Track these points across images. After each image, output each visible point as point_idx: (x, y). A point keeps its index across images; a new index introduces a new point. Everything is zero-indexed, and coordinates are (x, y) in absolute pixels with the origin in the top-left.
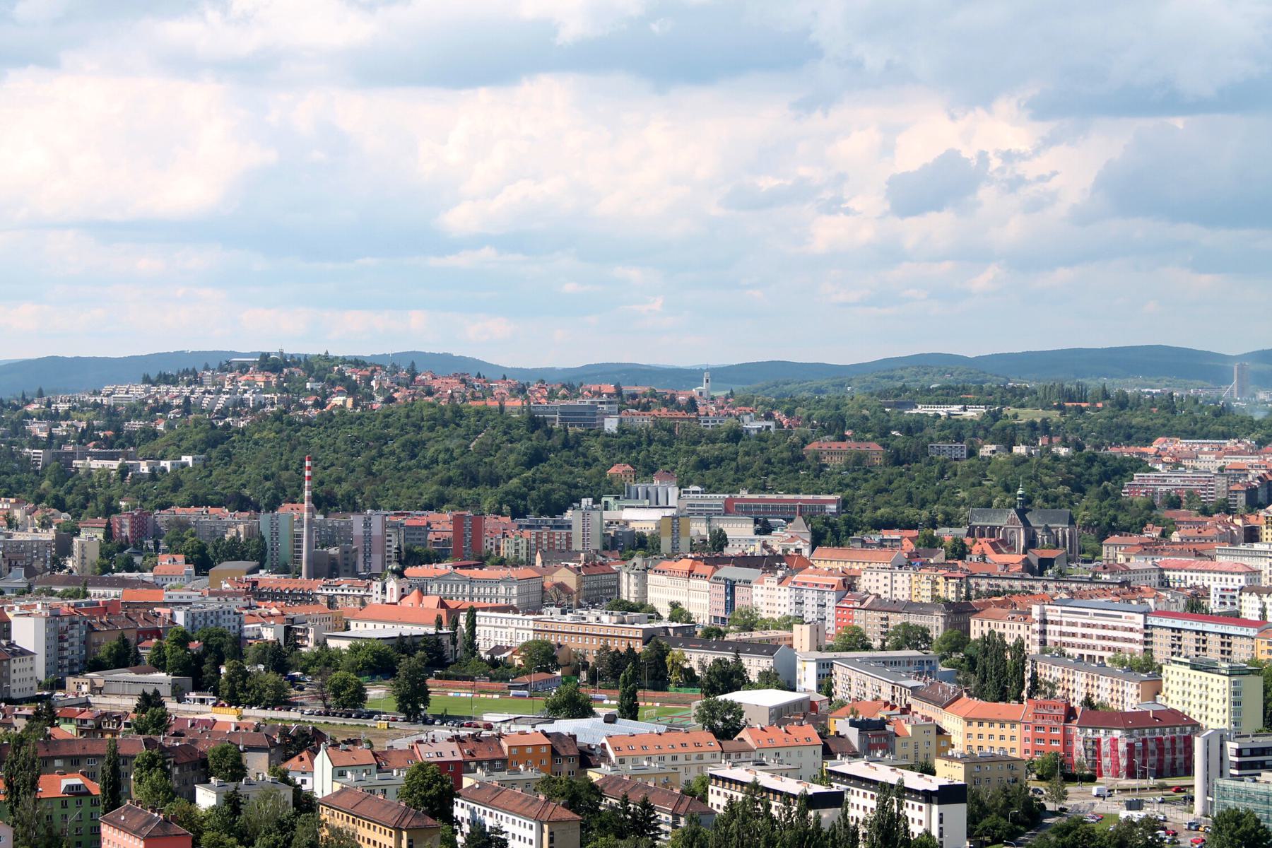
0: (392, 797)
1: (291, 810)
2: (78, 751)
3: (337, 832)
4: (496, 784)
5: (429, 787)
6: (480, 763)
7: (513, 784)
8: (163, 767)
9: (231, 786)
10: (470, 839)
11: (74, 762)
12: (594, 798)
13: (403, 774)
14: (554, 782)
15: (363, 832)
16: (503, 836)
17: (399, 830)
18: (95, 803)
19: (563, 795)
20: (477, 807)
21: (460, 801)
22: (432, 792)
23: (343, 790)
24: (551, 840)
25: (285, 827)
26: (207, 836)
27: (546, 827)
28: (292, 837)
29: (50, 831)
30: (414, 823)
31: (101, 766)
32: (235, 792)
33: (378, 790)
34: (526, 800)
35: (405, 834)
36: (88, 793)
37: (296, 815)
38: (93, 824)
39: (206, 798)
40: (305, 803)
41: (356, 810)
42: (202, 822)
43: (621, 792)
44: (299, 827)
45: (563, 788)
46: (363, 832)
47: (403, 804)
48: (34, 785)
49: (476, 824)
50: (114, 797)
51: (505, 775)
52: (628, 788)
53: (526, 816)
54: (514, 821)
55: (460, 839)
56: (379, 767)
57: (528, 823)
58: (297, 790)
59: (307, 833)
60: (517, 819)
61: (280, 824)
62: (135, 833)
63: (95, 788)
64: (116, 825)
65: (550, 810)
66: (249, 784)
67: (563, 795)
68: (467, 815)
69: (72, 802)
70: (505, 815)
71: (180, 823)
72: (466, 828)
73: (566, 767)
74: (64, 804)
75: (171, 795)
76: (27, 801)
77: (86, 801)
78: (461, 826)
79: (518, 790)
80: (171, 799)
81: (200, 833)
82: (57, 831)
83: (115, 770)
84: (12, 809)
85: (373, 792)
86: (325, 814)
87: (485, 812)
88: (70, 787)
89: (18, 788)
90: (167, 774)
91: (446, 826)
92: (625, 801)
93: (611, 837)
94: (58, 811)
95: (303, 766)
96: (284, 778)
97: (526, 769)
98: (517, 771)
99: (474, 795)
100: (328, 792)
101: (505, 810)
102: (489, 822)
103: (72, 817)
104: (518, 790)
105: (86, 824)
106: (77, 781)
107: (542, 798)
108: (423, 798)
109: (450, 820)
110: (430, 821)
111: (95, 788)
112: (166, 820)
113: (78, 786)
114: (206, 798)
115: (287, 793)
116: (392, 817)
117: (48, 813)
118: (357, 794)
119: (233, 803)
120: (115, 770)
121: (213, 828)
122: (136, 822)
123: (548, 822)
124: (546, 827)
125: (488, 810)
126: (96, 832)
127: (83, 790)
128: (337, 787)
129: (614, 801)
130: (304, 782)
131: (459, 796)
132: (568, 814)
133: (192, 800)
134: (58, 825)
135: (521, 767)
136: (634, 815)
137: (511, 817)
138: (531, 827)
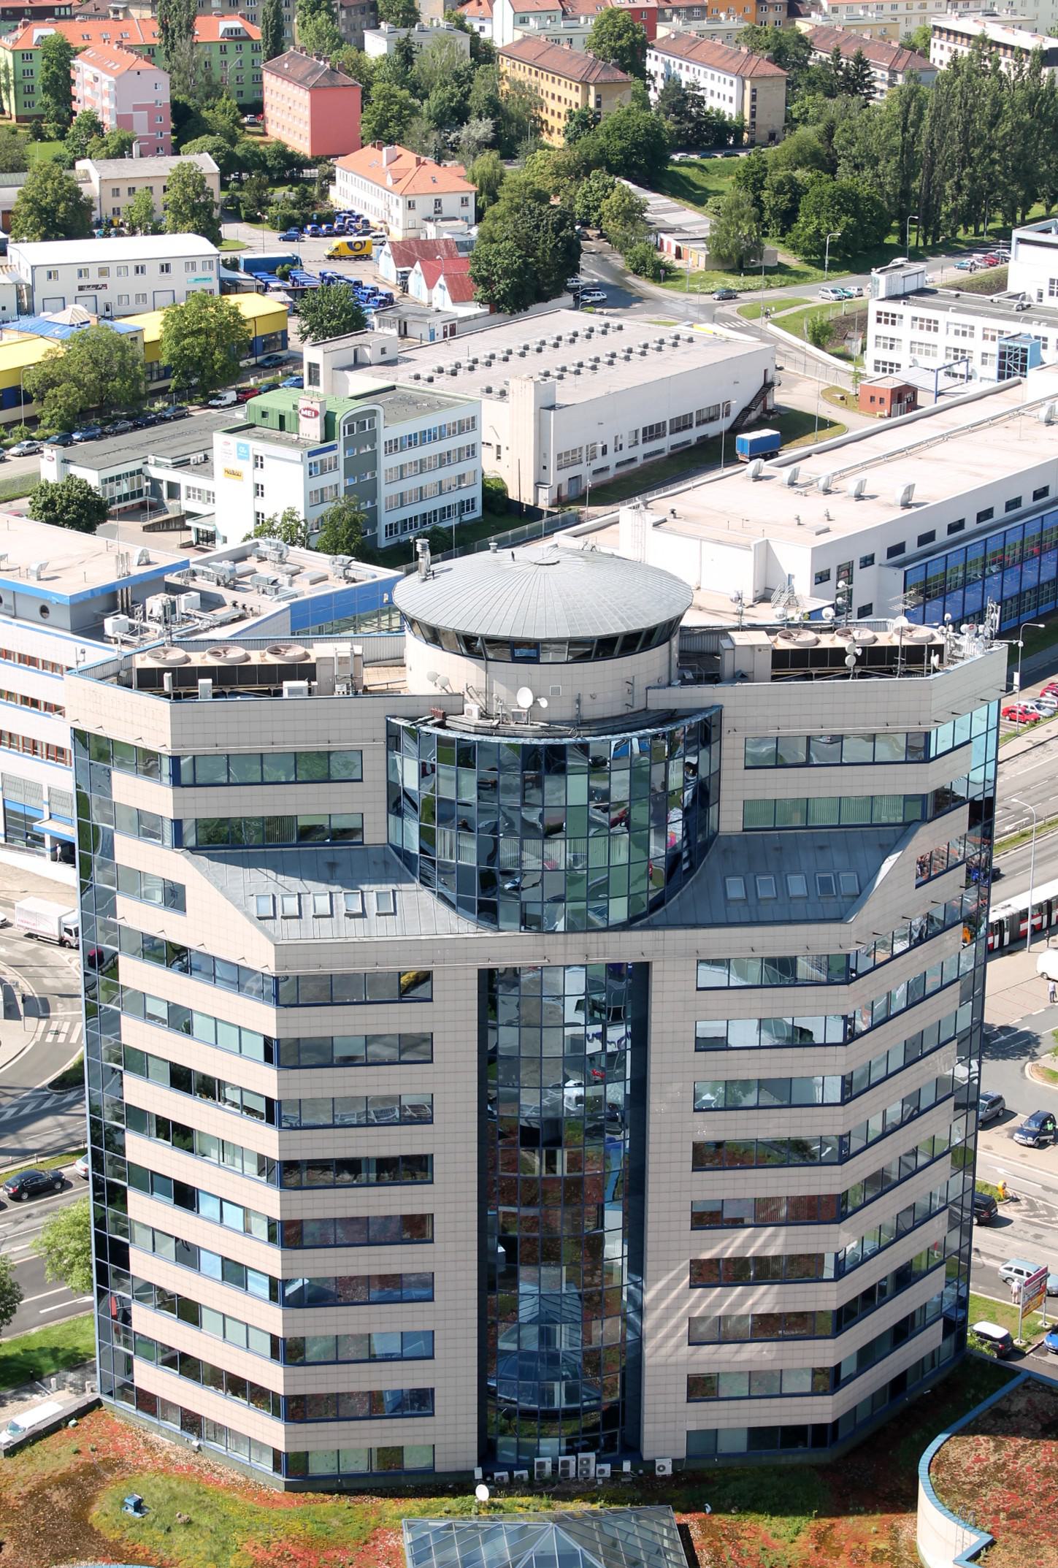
0: (579, 48)
1: (469, 61)
3: (518, 86)
4: (693, 34)
5: (620, 37)
6: (676, 10)
7: (714, 34)
8: (328, 10)
9: (403, 32)
10: (664, 95)
12: (802, 51)
13: (592, 22)
14: (758, 33)
15: (547, 85)
16: (700, 93)
17: (586, 84)
19: (768, 47)
20: (672, 60)
21: (653, 53)
22: (619, 43)
23: (525, 39)
24: (754, 98)
25: (462, 79)
26: (377, 88)
27: (748, 83)
28: (470, 91)
29: (209, 79)
30: (603, 78)
32: (407, 39)
33: (564, 40)
34: (727, 53)
35: (592, 89)
36: (248, 38)
37: (474, 66)
38: (255, 72)
39: (377, 45)
40: (483, 54)
41: (539, 62)
42: (372, 72)
43: (833, 45)
44: (477, 79)
45: (768, 39)
46: (547, 85)
47: (591, 56)
48: (190, 27)
49: (670, 79)
51: (703, 24)
52: (841, 40)
53: (727, 71)
54: (713, 77)
56: (564, 13)
57: (729, 78)
58: (475, 39)
59: (486, 86)
60: (717, 74)
61: (457, 76)
62: (300, 82)
65: (753, 64)
66: (422, 30)
67: (768, 47)
70: (703, 70)
71: (348, 73)
72: (660, 84)
73: (772, 16)
75: (338, 42)
76: (184, 45)
77: (247, 46)
78: (654, 81)
79: (718, 42)
80: (339, 46)
81: (369, 84)
82: (216, 79)
84: (167, 54)
85: (558, 41)
86: (505, 65)
87: (681, 66)
89: (173, 32)
91: (637, 81)
92: (837, 55)
93: (819, 95)
94: (216, 57)
95: (482, 11)
96: (461, 26)
97: (728, 18)
98: (717, 20)
99: (670, 48)
100: (508, 41)
101: (703, 64)
102: (686, 77)
103: (232, 65)
104: (718, 42)
105: (247, 73)
107: (744, 50)
108: (613, 49)
109: (641, 73)
110: (620, 75)
111: (256, 32)
112: (333, 70)
113: (238, 31)
115: (464, 42)
116: (578, 70)
117: (207, 59)
118: (540, 44)
119: (406, 53)
121: (384, 80)
122: (301, 71)
123: (750, 78)
124: (748, 83)
125: (685, 64)
127: (242, 34)
128: (518, 35)
129: (825, 56)
130: (482, 29)
131: (652, 47)
132: (773, 69)
133: (361, 48)
135: (722, 15)
136: (846, 72)
137: (710, 72)
138: (731, 83)
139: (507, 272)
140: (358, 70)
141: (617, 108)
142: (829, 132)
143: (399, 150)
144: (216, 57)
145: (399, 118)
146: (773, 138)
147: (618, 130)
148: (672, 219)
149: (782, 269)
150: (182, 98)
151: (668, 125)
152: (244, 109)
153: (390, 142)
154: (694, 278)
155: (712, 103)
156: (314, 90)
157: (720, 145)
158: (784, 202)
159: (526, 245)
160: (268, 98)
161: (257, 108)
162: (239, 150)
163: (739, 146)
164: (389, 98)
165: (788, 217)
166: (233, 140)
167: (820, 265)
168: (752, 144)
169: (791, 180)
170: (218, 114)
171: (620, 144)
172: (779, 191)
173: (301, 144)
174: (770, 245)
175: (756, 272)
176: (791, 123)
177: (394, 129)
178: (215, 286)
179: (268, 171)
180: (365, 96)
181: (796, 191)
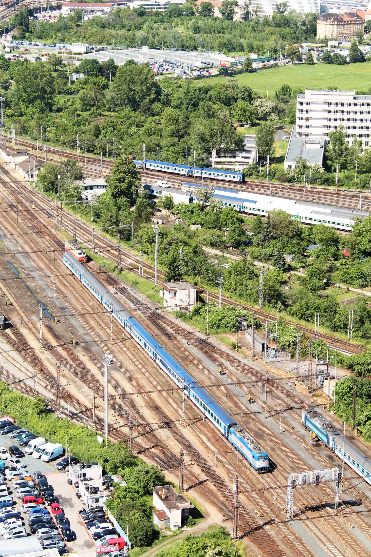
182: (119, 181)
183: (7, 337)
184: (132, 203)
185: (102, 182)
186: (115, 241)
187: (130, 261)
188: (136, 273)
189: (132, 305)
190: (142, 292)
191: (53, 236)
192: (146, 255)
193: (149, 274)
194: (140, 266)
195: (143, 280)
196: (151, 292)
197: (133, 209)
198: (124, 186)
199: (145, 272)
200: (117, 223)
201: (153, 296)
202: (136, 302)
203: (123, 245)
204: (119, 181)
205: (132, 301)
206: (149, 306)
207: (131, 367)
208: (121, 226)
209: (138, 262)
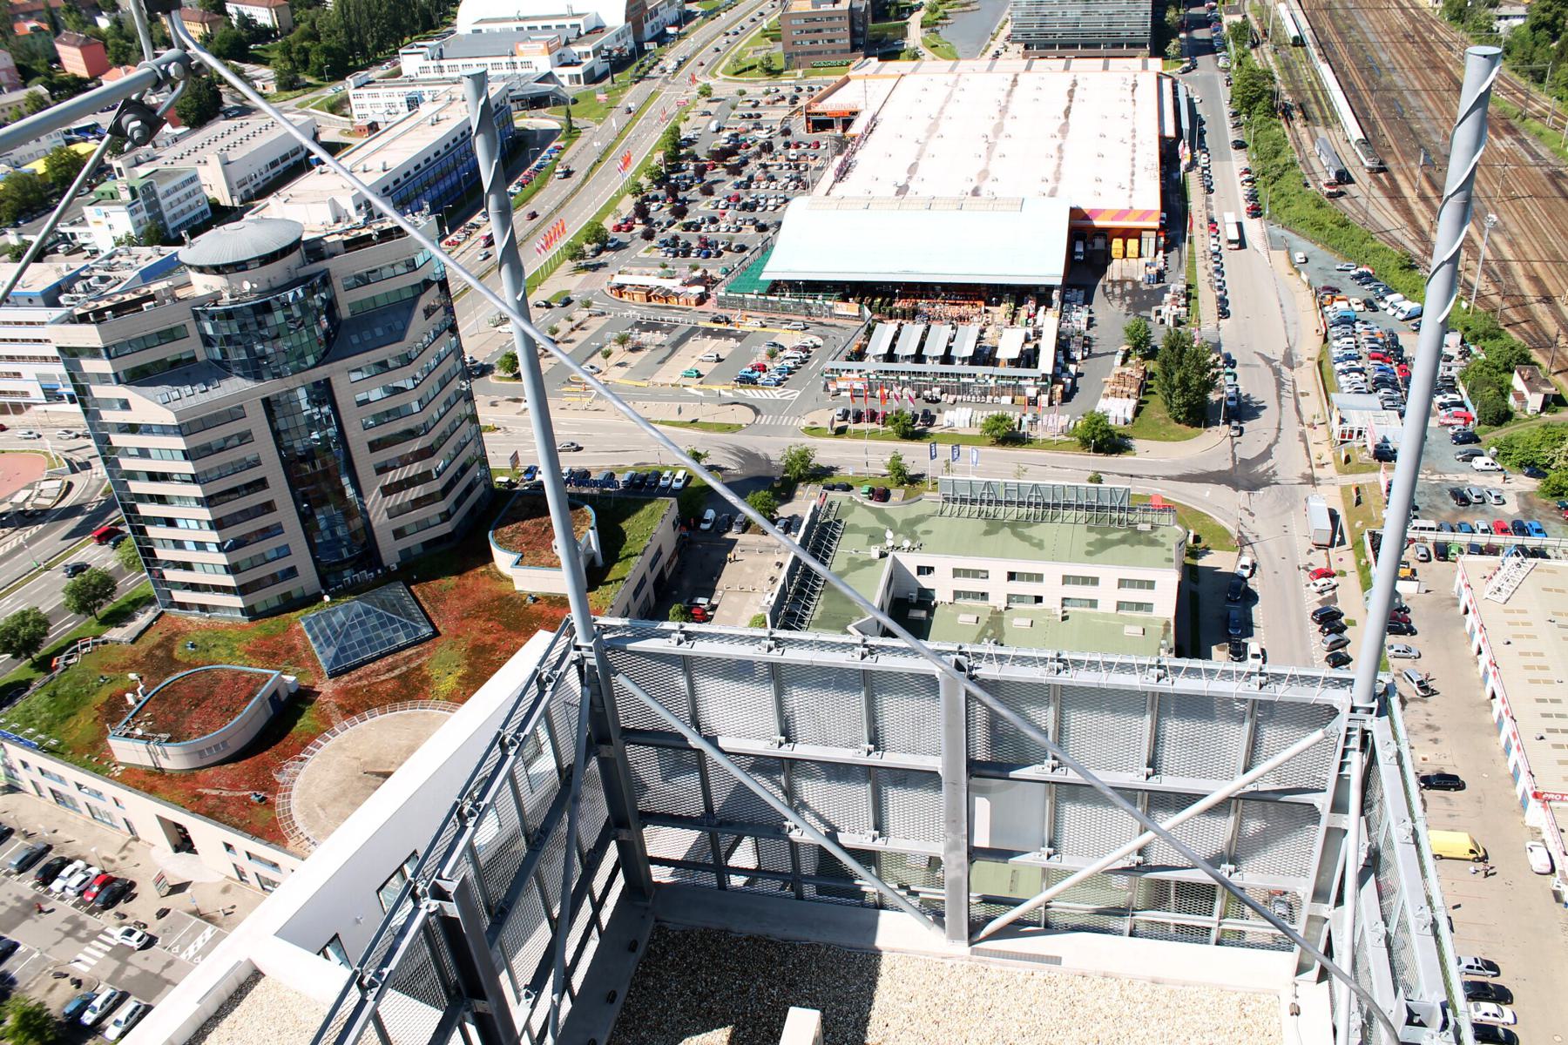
0: (196, 8)
2: (29, 9)
9: (114, 15)
10: (238, 21)
11: (29, 15)
17: (203, 23)
18: (48, 34)
26: (110, 42)
31: (45, 14)
36: (43, 30)
48: (12, 29)
49: (240, 14)
50: (56, 29)
55: (234, 23)
62: (74, 45)
63: (45, 26)
64: (62, 43)
68: (235, 11)
69: (36, 36)
72: (236, 17)
74: (32, 36)
75: (85, 24)
76: (12, 38)
81: (105, 41)
83: (52, 16)
88: (32, 29)
90: (79, 13)
94: (30, 40)
102: (246, 13)
103: (39, 41)
106: (34, 24)
109: (226, 13)
111: (45, 26)
114: (104, 23)
119: (118, 23)
120: (52, 16)
122: (72, 40)
126: (54, 48)
133: (96, 25)
134: (33, 48)
139: (192, 110)
140: (99, 35)
141: (220, 30)
142: (313, 24)
143: (128, 67)
144: (30, 40)
145: (123, 53)
146: (290, 31)
147: (223, 40)
148: (257, 74)
149: (309, 85)
150: (20, 62)
151: (243, 34)
152: (52, 62)
153: (123, 64)
154: (273, 96)
155: (260, 21)
156: (81, 47)
157: (270, 39)
158: (302, 57)
159: (196, 96)
160: (61, 55)
161: (58, 60)
162: (55, 81)
163: (277, 37)
164: (117, 45)
165: (305, 63)
166: (50, 77)
167: (324, 80)
168: (282, 35)
169: (302, 47)
170: (39, 65)
171: (225, 46)
172: (298, 52)
173: (83, 73)
174: (301, 76)
175: (297, 89)
176: (296, 24)
177: (123, 58)
178: (63, 143)
179: (72, 88)
180: (106, 47)
181: (306, 51)
182: (1544, 10)
183: (1379, 181)
184: (1555, 37)
185: (1521, 10)
186: (1523, 83)
187: (1538, 107)
188: (1544, 123)
189: (1530, 159)
190: (1546, 145)
191: (1449, 73)
192: (1558, 102)
193: (1559, 124)
194: (1549, 114)
195: (1549, 131)
196: (1556, 146)
197: (1554, 45)
198: (1548, 16)
199: (1554, 121)
200: (1530, 61)
201: (1558, 151)
202: (1535, 156)
203: (1534, 89)
204: (1544, 10)
205: (1531, 155)
206: (1551, 161)
207: (1515, 230)
208: (1535, 66)
209: (1547, 109)
